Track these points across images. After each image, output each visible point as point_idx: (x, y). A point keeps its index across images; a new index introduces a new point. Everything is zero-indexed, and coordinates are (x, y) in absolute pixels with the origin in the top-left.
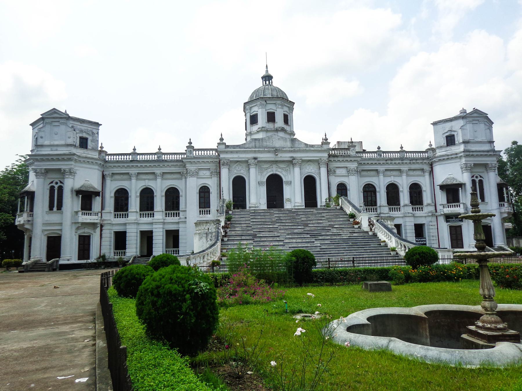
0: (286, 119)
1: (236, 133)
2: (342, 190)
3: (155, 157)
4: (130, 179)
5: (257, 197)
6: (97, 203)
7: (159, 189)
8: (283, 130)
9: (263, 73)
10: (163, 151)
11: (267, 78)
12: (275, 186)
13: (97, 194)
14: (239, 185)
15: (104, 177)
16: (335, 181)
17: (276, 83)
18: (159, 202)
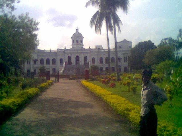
0: (82, 41)
1: (68, 45)
2: (93, 59)
3: (50, 51)
4: (44, 56)
5: (73, 61)
6: (37, 62)
7: (51, 59)
8: (80, 44)
9: (76, 29)
10: (52, 49)
11: (77, 30)
12: (77, 58)
13: (37, 60)
14: (69, 58)
15: (38, 56)
16: (92, 57)
17: (79, 31)
18: (51, 62)
